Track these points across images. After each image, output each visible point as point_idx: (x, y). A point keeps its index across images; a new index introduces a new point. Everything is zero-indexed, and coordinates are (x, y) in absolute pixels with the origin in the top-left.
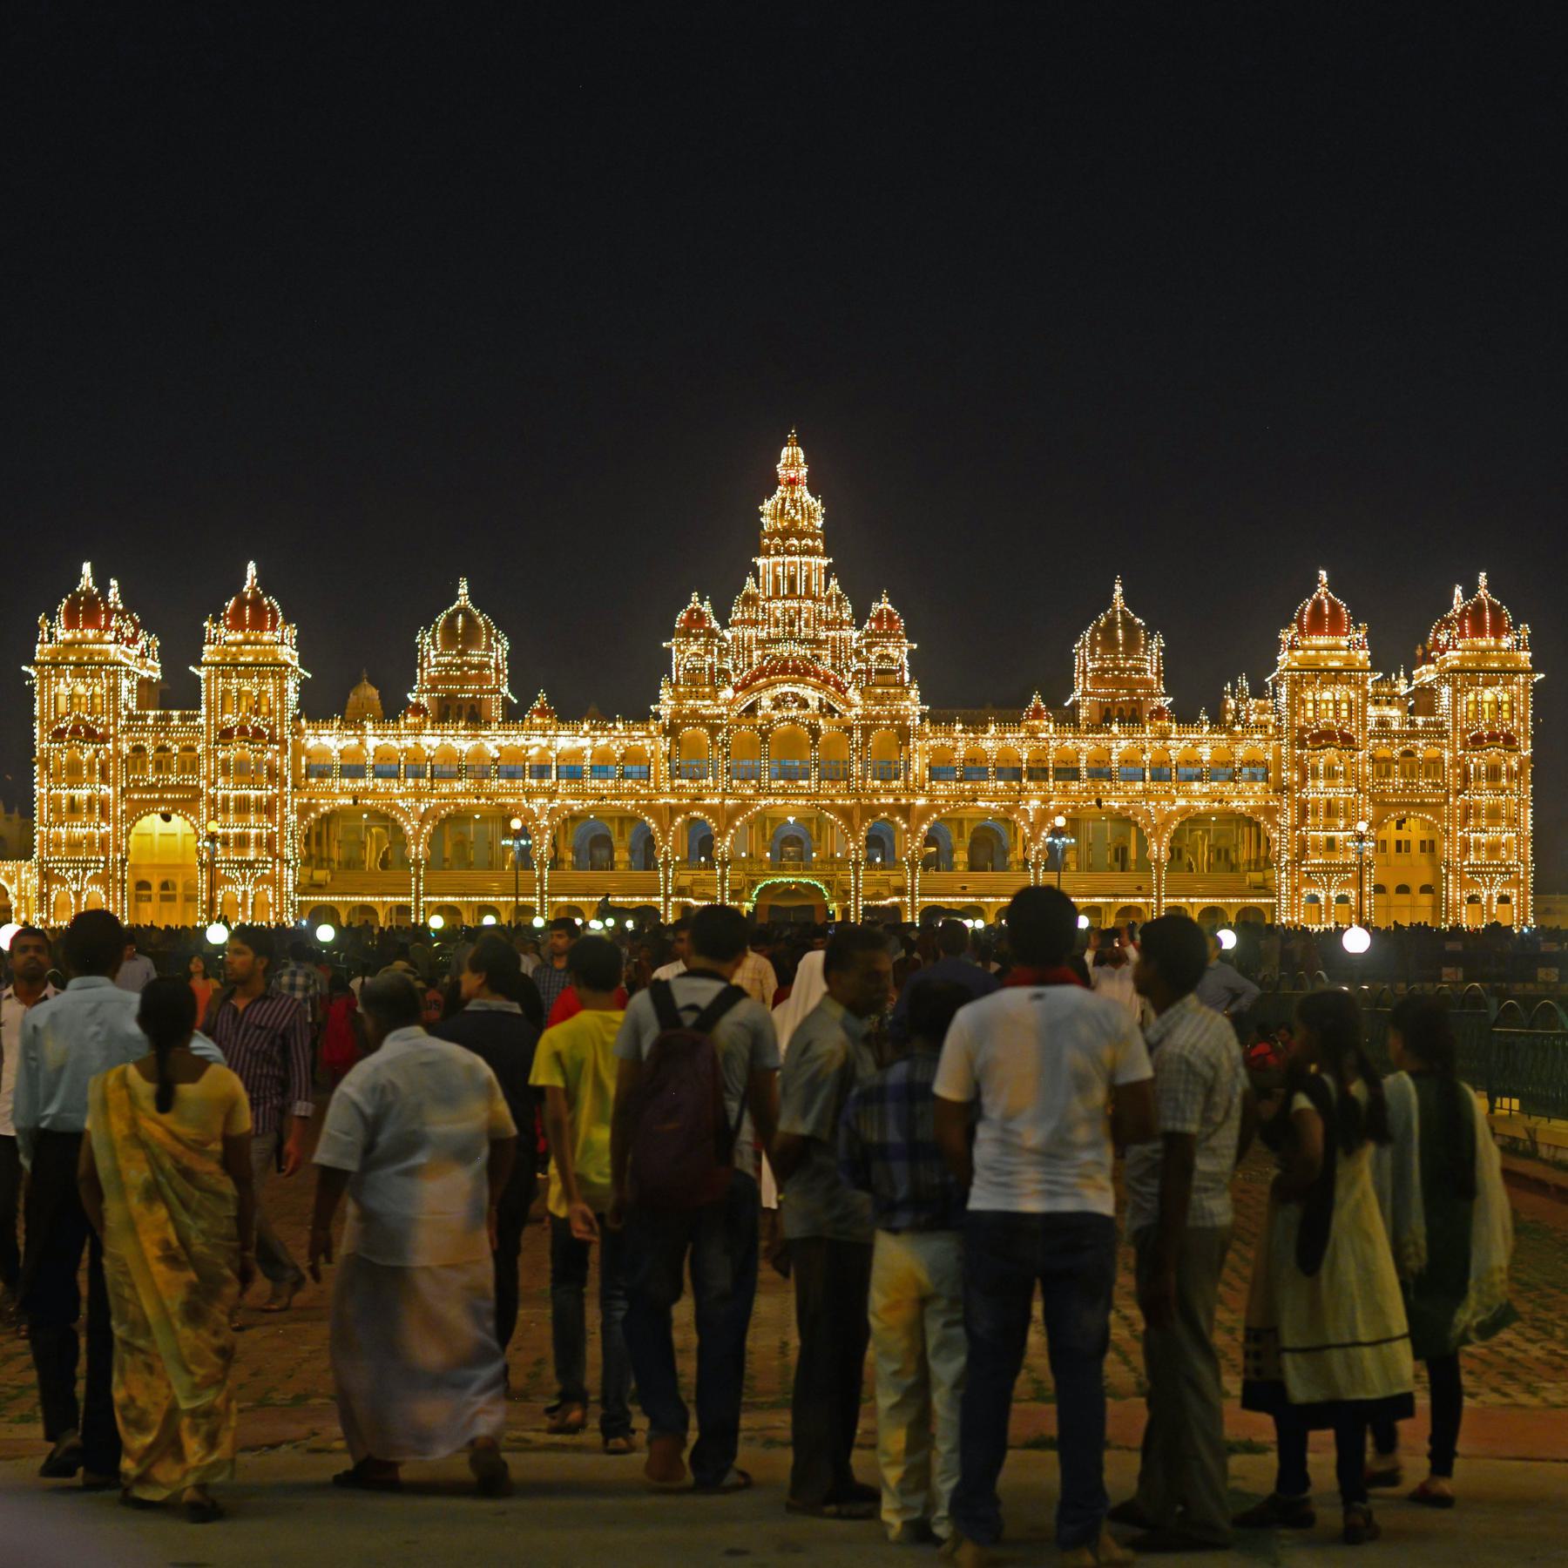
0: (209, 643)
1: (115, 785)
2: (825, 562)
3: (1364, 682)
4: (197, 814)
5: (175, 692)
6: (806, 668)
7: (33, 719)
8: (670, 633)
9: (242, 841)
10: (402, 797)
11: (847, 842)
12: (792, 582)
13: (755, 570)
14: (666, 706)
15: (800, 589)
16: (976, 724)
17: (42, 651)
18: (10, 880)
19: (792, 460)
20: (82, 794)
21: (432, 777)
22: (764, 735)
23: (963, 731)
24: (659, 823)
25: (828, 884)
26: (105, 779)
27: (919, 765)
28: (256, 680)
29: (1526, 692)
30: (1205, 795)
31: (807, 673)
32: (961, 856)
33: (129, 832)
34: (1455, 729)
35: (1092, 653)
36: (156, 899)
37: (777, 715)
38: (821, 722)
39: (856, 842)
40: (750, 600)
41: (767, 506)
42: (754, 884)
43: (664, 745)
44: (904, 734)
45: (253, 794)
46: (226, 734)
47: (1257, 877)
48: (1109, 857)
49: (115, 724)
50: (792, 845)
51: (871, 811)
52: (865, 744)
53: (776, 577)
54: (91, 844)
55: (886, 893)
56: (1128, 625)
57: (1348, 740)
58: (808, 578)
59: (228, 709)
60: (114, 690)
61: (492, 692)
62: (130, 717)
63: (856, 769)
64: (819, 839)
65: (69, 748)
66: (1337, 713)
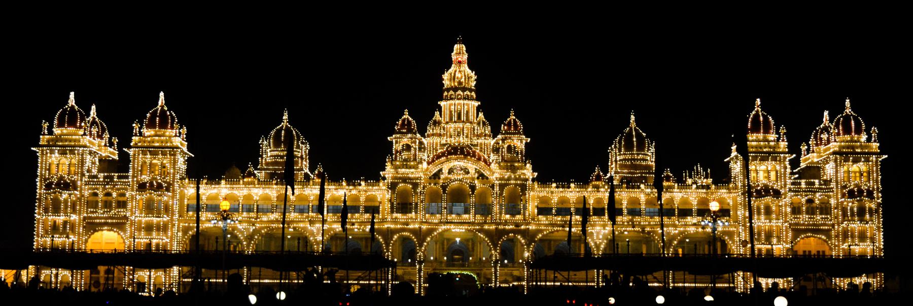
0: (136, 135)
1: (80, 215)
2: (477, 104)
3: (784, 160)
4: (125, 231)
5: (118, 166)
6: (468, 152)
8: (393, 132)
10: (240, 222)
11: (490, 250)
14: (389, 172)
15: (463, 118)
16: (564, 182)
17: (44, 139)
19: (459, 52)
20: (60, 219)
21: (257, 212)
23: (557, 187)
25: (478, 275)
26: (74, 211)
27: (532, 208)
28: (160, 156)
29: (877, 166)
30: (694, 225)
31: (469, 154)
33: (86, 241)
34: (837, 187)
35: (620, 151)
38: (476, 182)
39: (496, 250)
40: (437, 123)
41: (446, 76)
46: (142, 187)
49: (81, 180)
50: (458, 253)
52: (501, 194)
53: (451, 112)
55: (510, 280)
56: (639, 135)
57: (777, 194)
58: (468, 112)
59: (144, 172)
60: (82, 162)
61: (298, 170)
62: (90, 177)
63: (496, 209)
64: (473, 248)
65: (55, 193)
66: (768, 177)
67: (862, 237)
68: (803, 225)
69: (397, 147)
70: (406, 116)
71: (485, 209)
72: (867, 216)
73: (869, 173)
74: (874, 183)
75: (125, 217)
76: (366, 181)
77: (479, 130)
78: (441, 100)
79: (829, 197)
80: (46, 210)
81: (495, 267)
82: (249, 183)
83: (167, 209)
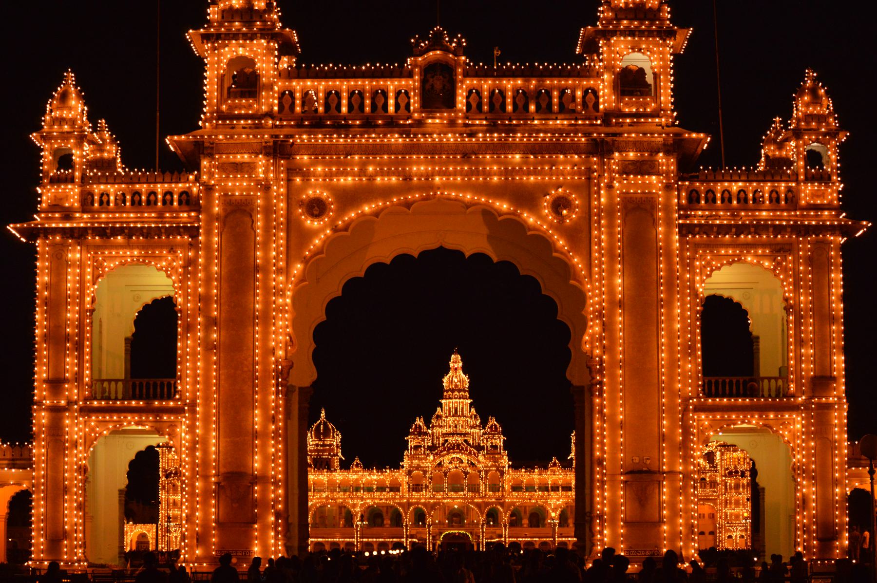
2: (469, 401)
8: (408, 434)
12: (456, 409)
13: (441, 405)
14: (406, 463)
15: (459, 413)
16: (530, 467)
18: (149, 531)
19: (456, 361)
22: (445, 474)
25: (471, 533)
32: (525, 521)
37: (451, 466)
40: (439, 417)
41: (445, 380)
42: (441, 533)
43: (406, 479)
50: (456, 517)
51: (488, 504)
53: (450, 408)
58: (463, 408)
63: (482, 488)
67: (737, 504)
69: (411, 444)
71: (474, 489)
73: (744, 459)
76: (390, 469)
77: (471, 422)
78: (442, 399)
79: (716, 476)
80: (168, 492)
81: (482, 528)
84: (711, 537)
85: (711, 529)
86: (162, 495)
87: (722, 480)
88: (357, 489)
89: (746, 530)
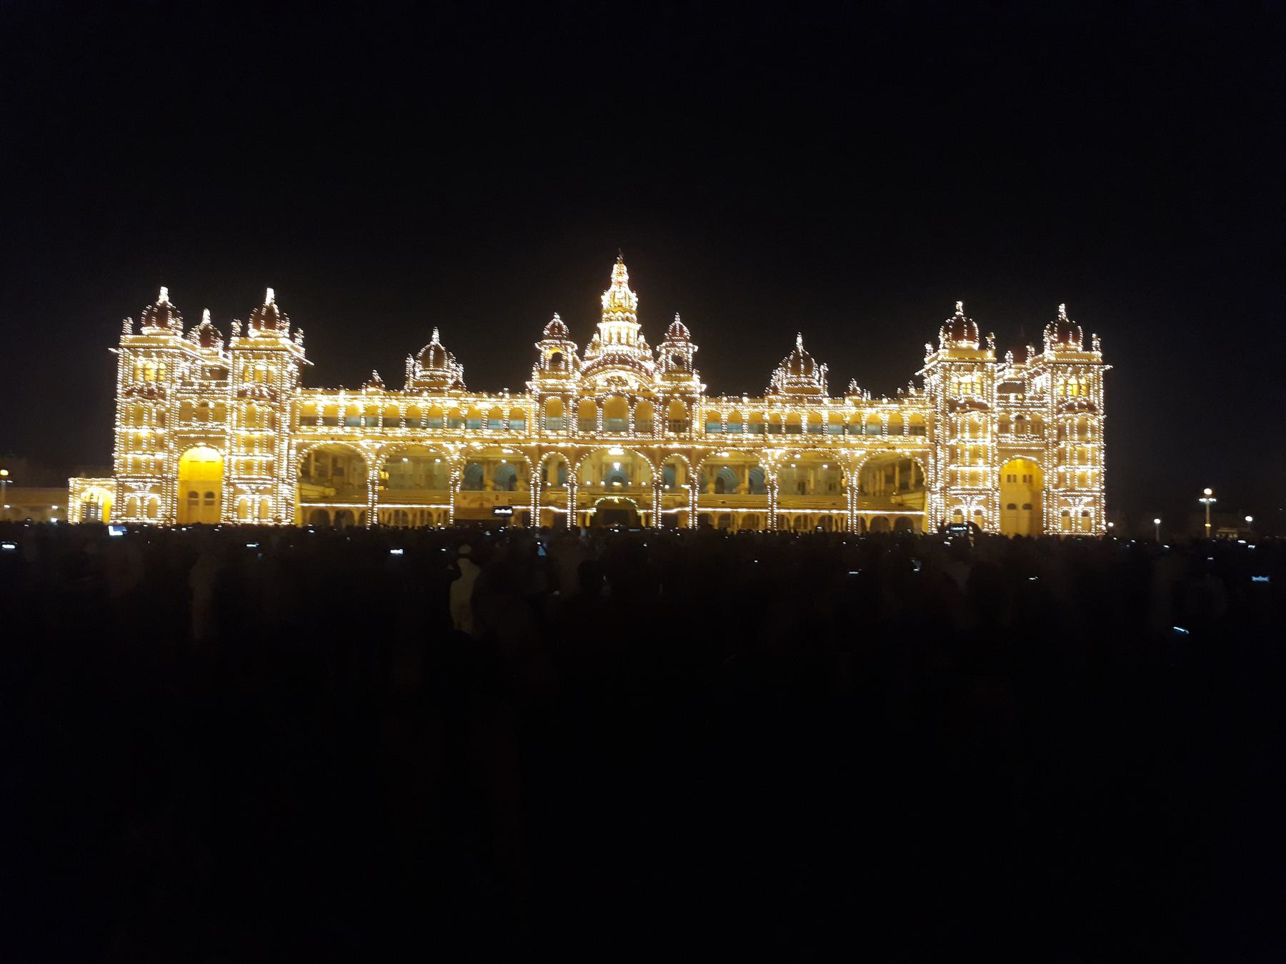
2: (638, 327)
7: (116, 382)
9: (249, 467)
14: (534, 384)
15: (623, 341)
19: (620, 273)
20: (144, 432)
23: (729, 401)
24: (531, 458)
25: (637, 500)
27: (697, 425)
33: (178, 460)
36: (201, 504)
42: (594, 500)
44: (691, 401)
45: (257, 435)
46: (242, 394)
47: (899, 499)
48: (795, 487)
51: (667, 453)
54: (148, 466)
57: (982, 407)
67: (1082, 458)
68: (1013, 445)
69: (547, 353)
70: (557, 318)
71: (645, 426)
72: (1089, 435)
74: (1098, 399)
75: (223, 431)
76: (510, 392)
78: (600, 321)
82: (373, 394)
83: (273, 423)
84: (1026, 513)
85: (1026, 498)
86: (121, 429)
87: (1054, 421)
88: (455, 424)
89: (1094, 503)
